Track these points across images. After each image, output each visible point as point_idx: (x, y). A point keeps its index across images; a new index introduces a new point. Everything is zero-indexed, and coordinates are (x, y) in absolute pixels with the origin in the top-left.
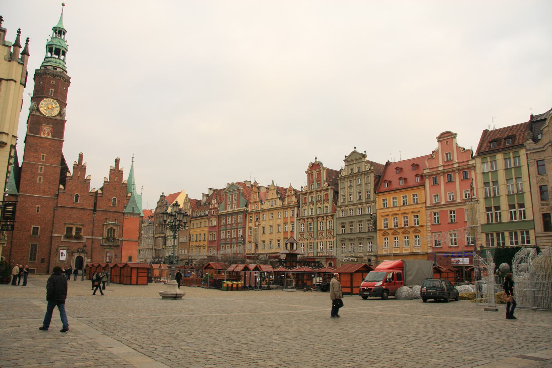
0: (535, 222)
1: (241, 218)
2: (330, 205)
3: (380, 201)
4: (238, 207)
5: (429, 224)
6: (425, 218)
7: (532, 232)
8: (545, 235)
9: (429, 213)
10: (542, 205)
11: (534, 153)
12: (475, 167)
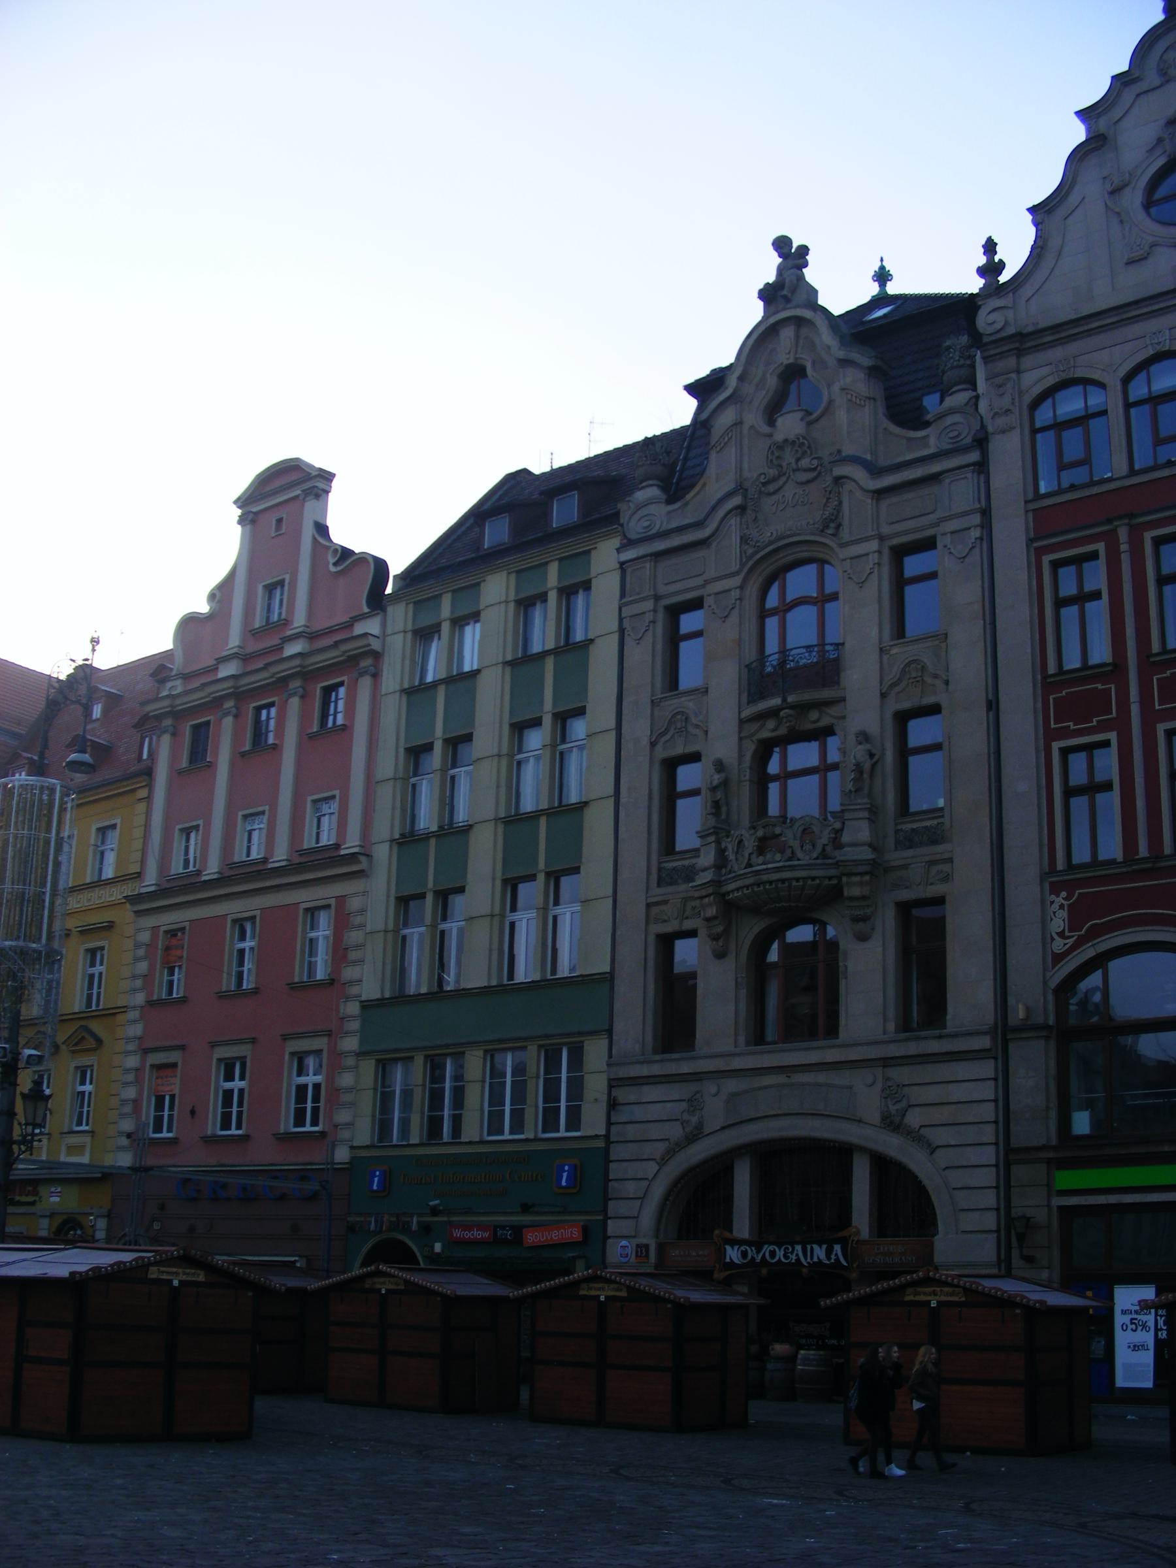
0: (621, 988)
5: (140, 998)
7: (595, 1052)
8: (656, 1069)
9: (145, 937)
10: (665, 878)
11: (657, 556)
12: (377, 656)
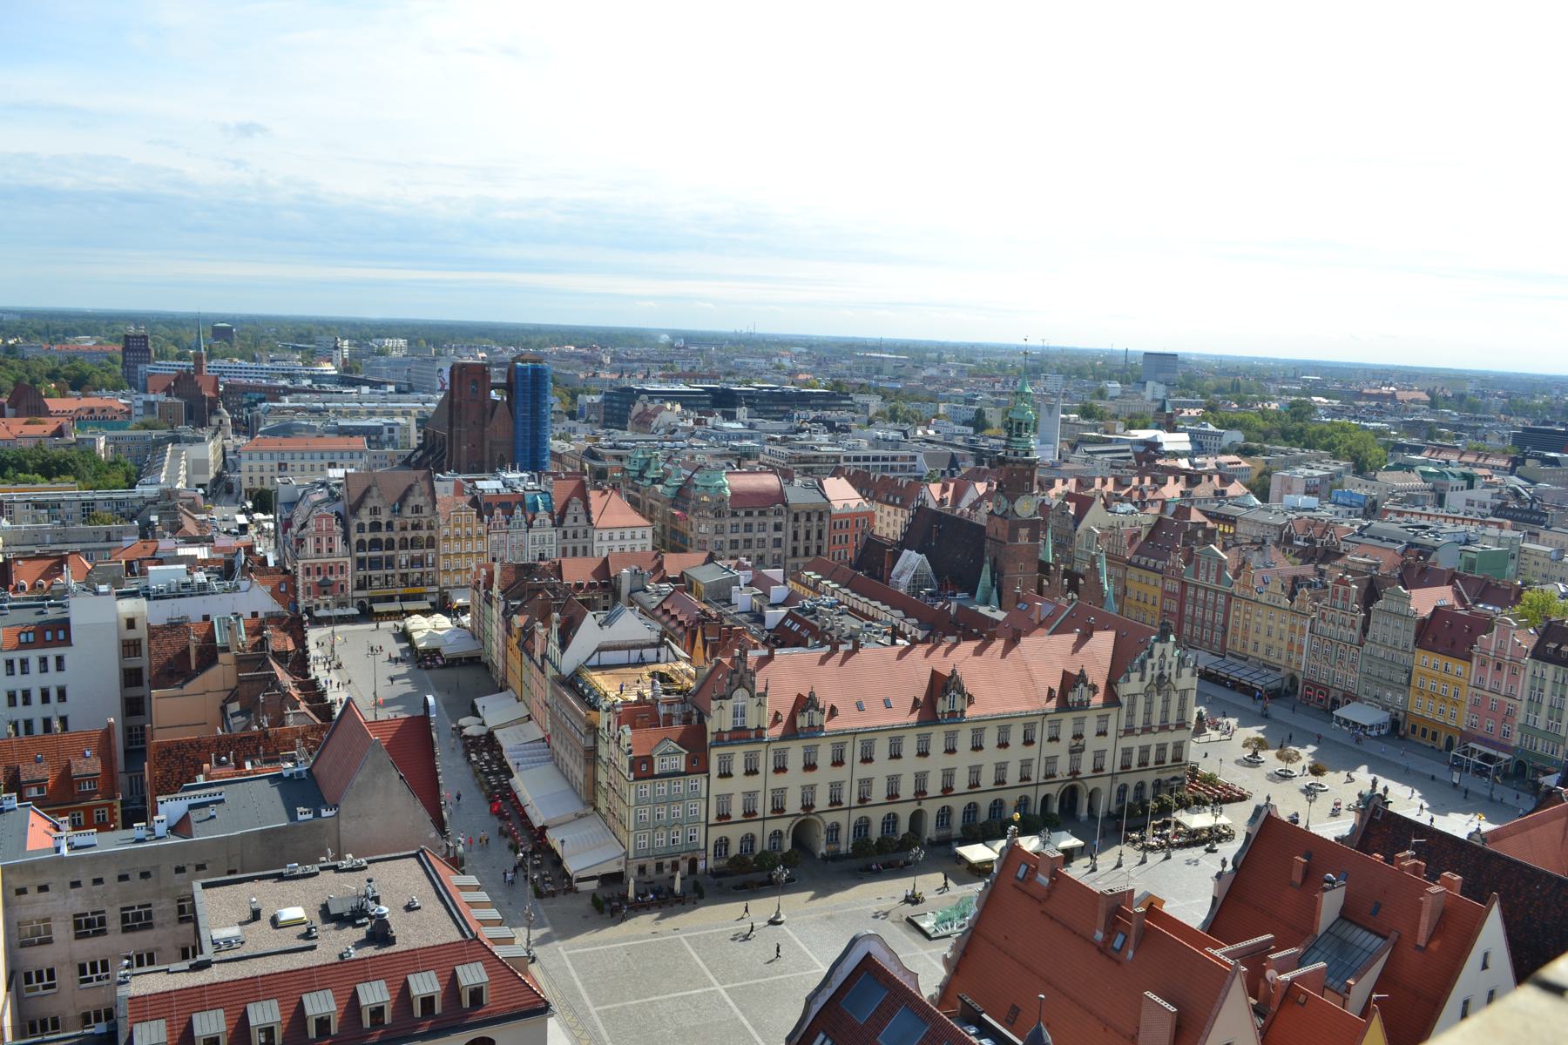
1: (1222, 600)
2: (1356, 634)
3: (1420, 653)
4: (1218, 582)
6: (1466, 694)
